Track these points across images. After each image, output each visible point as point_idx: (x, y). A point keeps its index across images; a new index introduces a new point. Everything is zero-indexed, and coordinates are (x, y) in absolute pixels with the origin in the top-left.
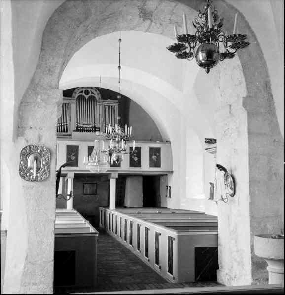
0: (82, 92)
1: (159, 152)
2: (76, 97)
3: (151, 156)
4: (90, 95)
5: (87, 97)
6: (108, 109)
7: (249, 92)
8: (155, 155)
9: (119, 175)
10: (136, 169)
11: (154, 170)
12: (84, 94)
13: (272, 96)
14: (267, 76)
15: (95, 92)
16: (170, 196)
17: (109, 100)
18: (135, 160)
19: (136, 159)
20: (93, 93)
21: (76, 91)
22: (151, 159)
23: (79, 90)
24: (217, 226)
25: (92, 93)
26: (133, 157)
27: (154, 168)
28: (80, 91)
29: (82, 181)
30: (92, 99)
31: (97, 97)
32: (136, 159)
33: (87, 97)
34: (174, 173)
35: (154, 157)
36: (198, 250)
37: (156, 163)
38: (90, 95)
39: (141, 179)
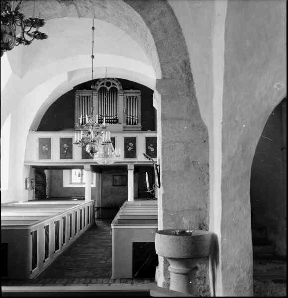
0: (103, 84)
2: (98, 90)
4: (112, 86)
5: (108, 88)
6: (130, 100)
7: (163, 73)
12: (105, 86)
13: (191, 76)
14: (187, 54)
15: (116, 84)
17: (131, 91)
19: (152, 150)
20: (115, 85)
21: (97, 83)
23: (100, 82)
24: (157, 220)
25: (113, 84)
26: (149, 147)
28: (101, 83)
29: (111, 173)
30: (114, 90)
31: (118, 88)
32: (152, 150)
33: (108, 88)
36: (136, 245)
38: (112, 86)
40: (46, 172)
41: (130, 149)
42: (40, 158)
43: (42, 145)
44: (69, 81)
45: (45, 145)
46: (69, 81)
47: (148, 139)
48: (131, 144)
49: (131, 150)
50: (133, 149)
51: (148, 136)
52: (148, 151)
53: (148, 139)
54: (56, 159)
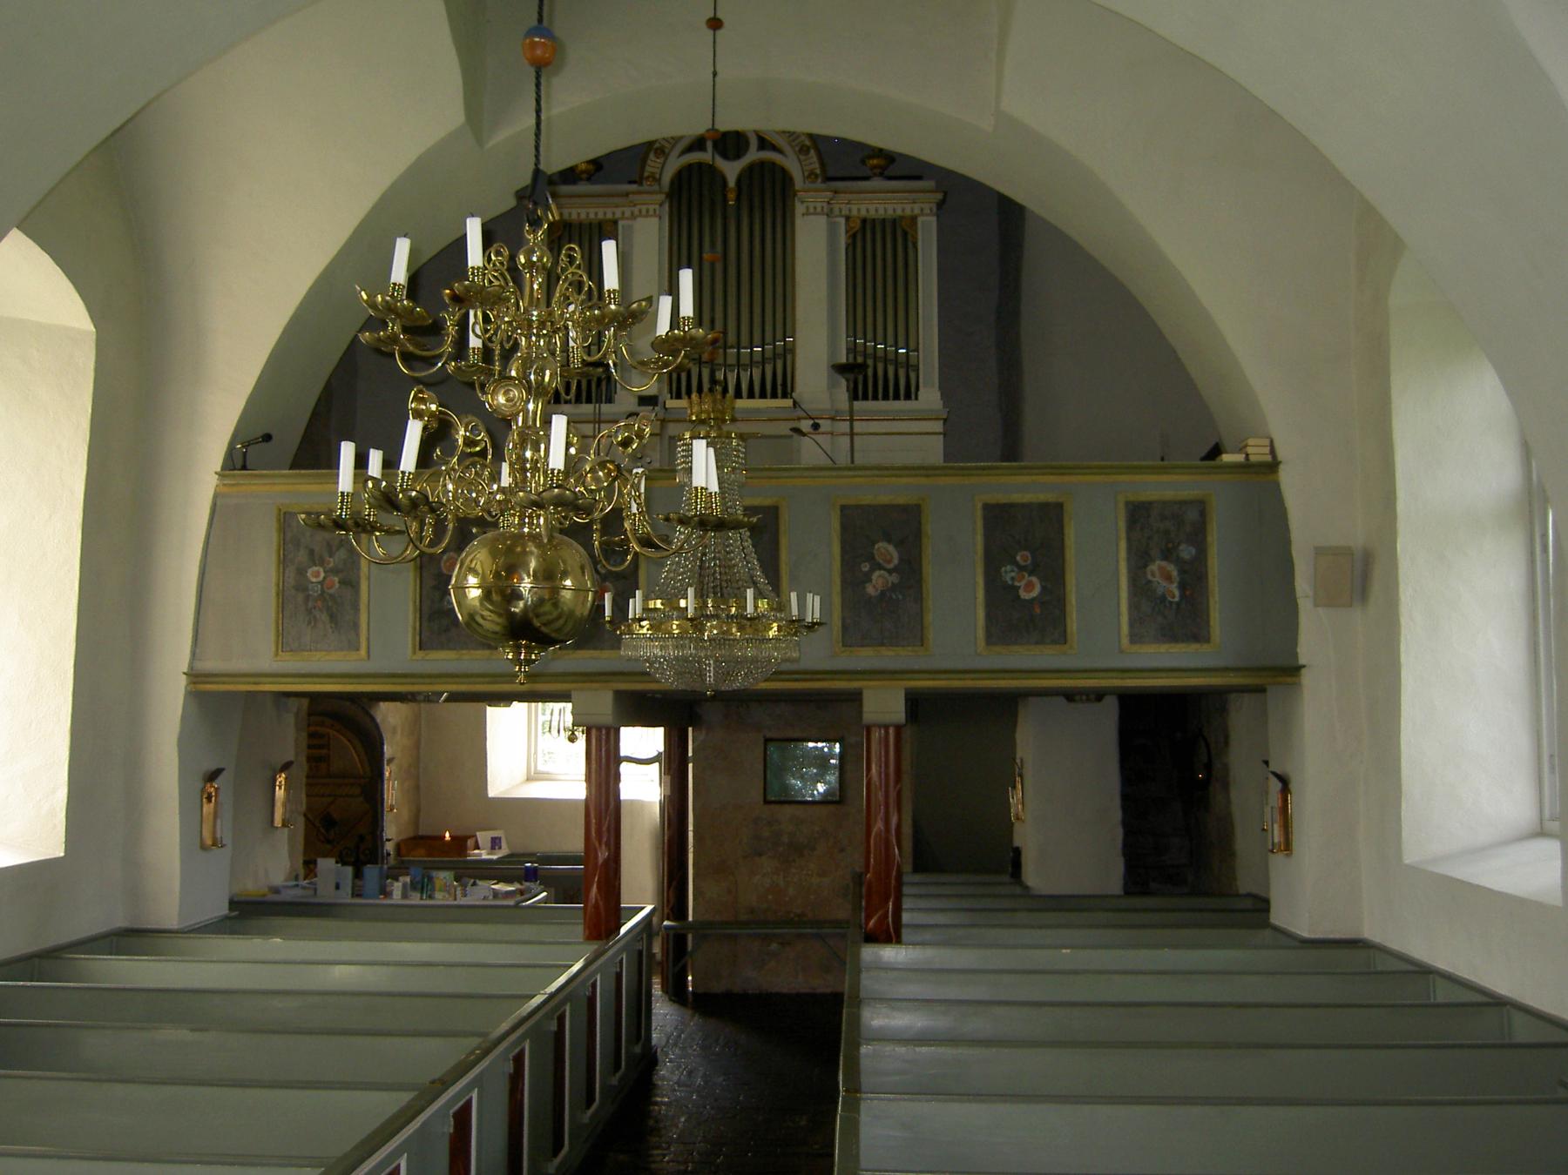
1: (1198, 535)
3: (1140, 559)
8: (1167, 555)
9: (915, 702)
10: (1026, 661)
11: (1166, 664)
16: (1287, 846)
18: (1024, 595)
19: (1030, 589)
22: (1140, 588)
26: (1008, 573)
27: (1164, 648)
32: (1030, 589)
34: (1307, 678)
35: (1164, 577)
37: (1183, 618)
39: (1108, 717)
40: (390, 716)
41: (878, 582)
42: (284, 643)
43: (302, 556)
44: (480, 141)
45: (322, 563)
46: (480, 141)
47: (998, 517)
48: (887, 551)
49: (883, 593)
50: (894, 587)
51: (1002, 498)
52: (1000, 596)
53: (998, 517)
54: (380, 643)
